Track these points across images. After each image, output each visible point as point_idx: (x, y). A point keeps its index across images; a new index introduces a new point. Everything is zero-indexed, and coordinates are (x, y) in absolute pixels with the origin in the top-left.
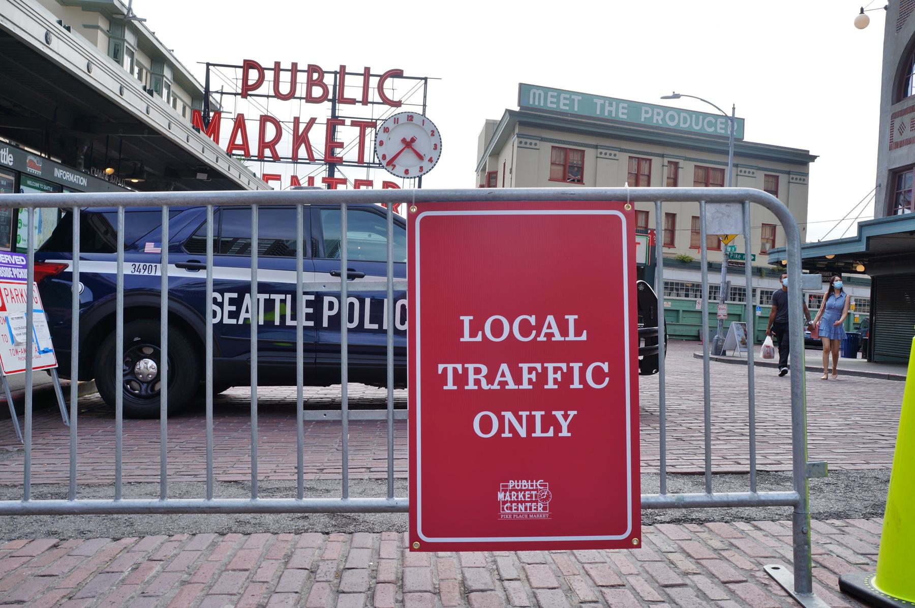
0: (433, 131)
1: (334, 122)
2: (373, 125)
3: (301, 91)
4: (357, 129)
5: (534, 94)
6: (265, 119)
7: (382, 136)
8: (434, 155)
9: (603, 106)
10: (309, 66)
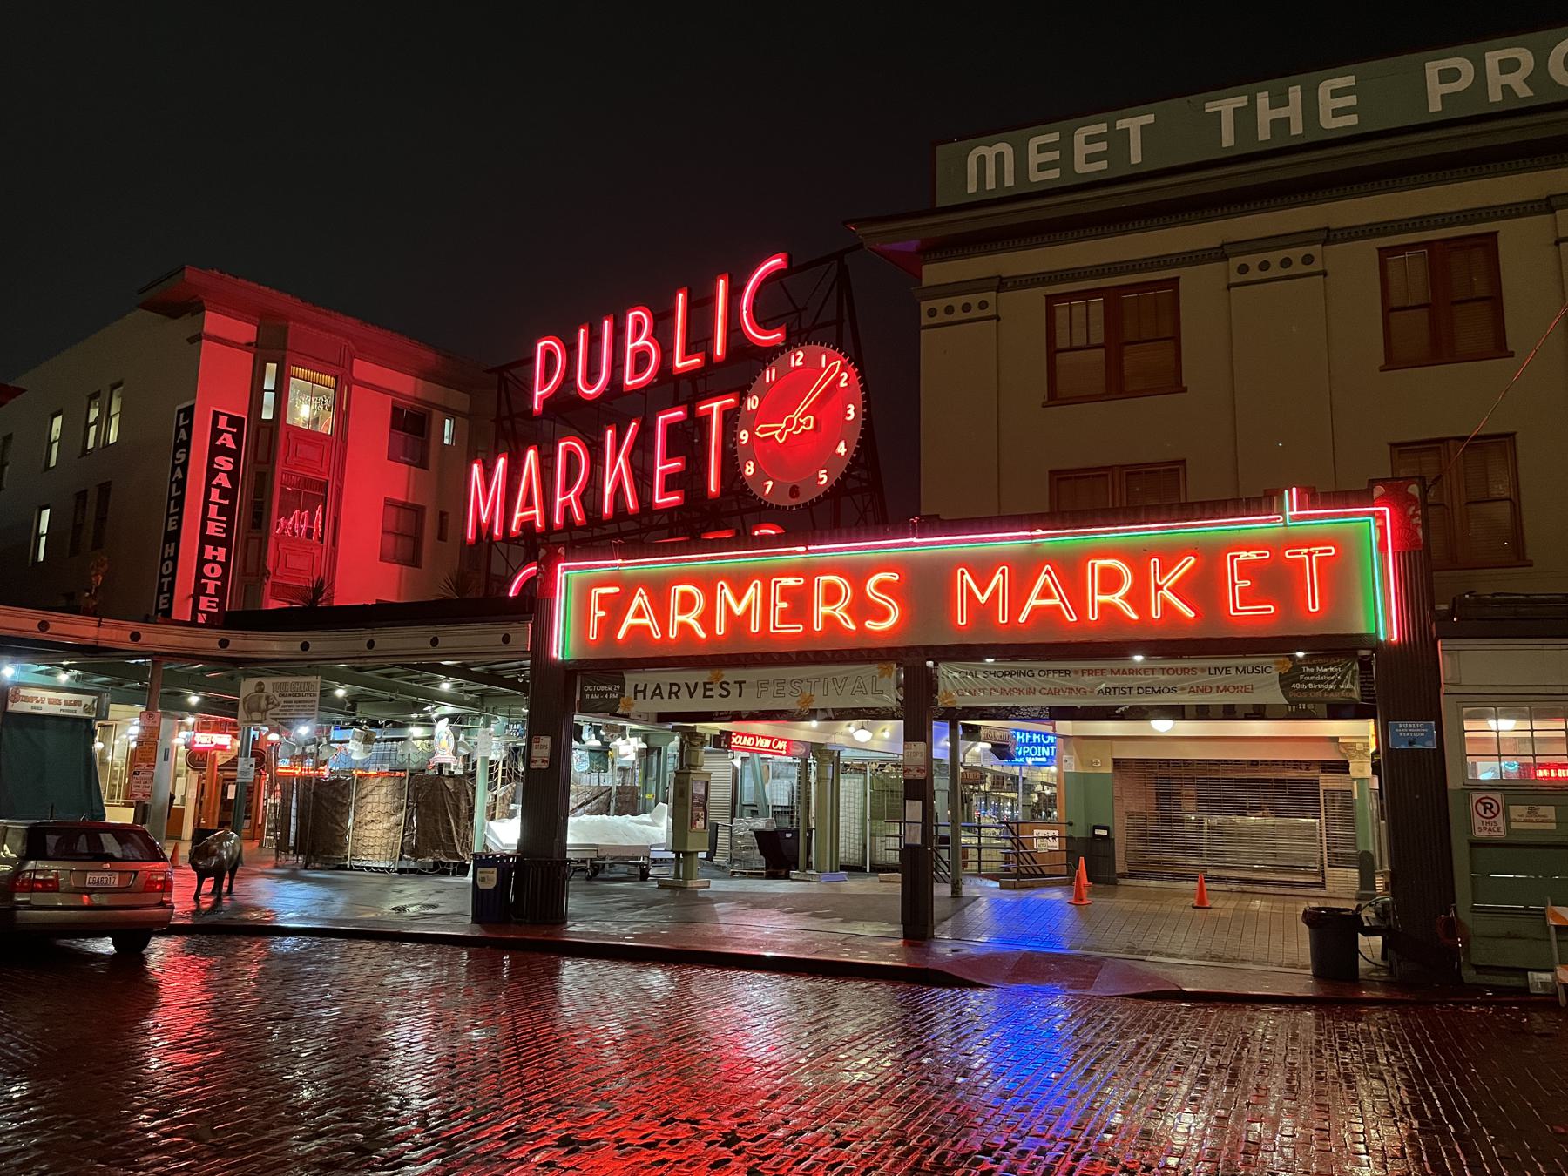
5: (982, 160)
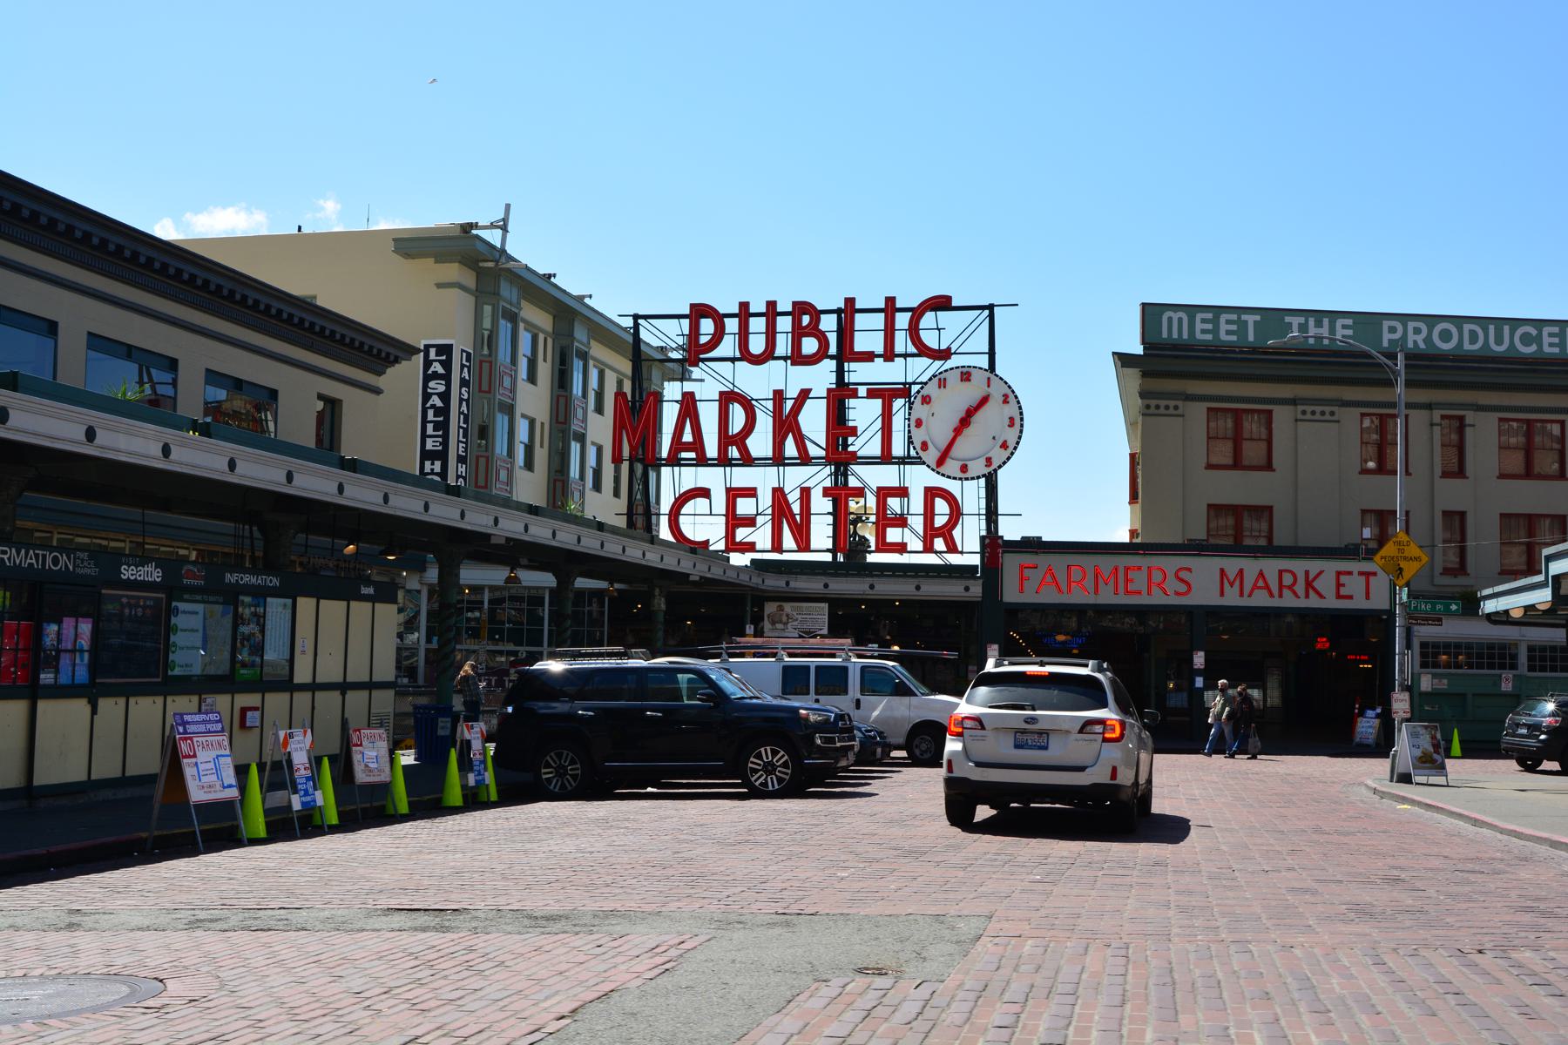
0: (1006, 396)
1: (840, 395)
2: (904, 391)
3: (783, 346)
4: (879, 401)
5: (1170, 319)
6: (728, 398)
7: (920, 410)
8: (1011, 438)
9: (1303, 328)
10: (795, 304)
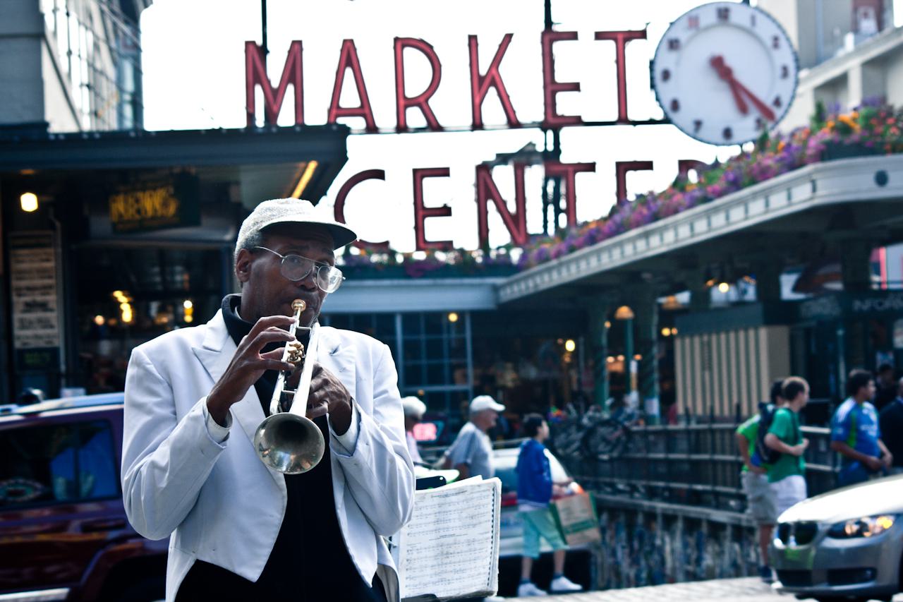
0: (776, 39)
